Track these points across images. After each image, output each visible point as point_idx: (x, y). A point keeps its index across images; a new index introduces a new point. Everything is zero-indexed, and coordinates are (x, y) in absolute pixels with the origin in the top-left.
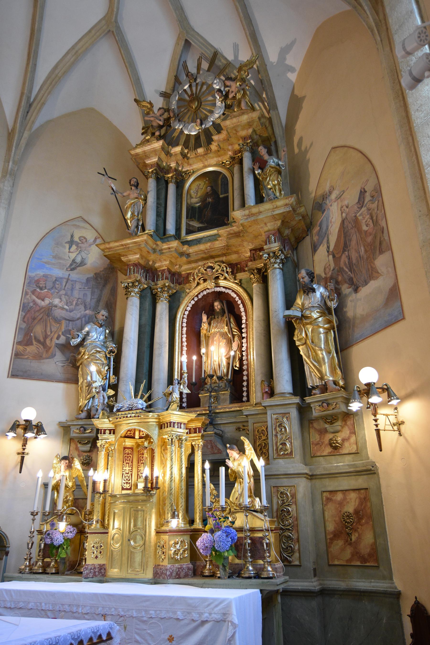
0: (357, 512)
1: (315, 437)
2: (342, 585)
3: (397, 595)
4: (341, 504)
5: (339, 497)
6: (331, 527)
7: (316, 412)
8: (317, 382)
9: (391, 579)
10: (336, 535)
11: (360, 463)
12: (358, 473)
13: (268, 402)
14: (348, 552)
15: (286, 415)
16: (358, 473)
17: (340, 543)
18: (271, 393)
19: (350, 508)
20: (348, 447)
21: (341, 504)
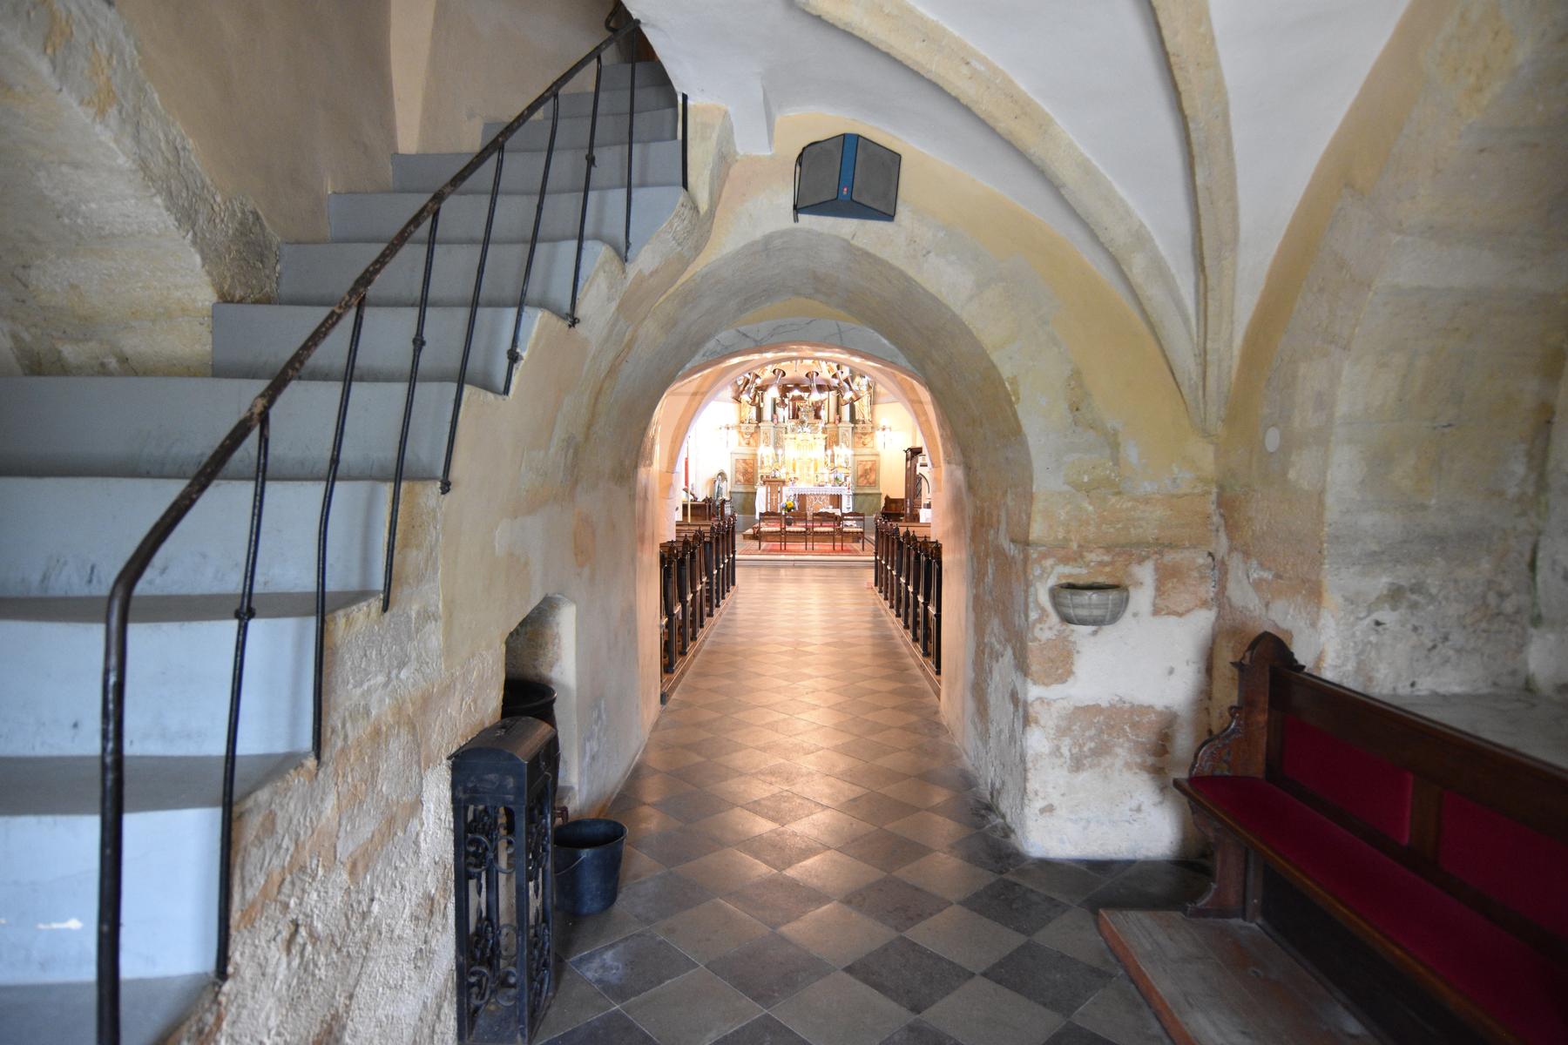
0: (870, 469)
1: (857, 440)
2: (862, 492)
3: (881, 494)
4: (865, 465)
5: (864, 463)
6: (860, 473)
7: (859, 431)
8: (861, 418)
9: (879, 489)
10: (861, 476)
11: (874, 451)
12: (873, 455)
13: (840, 425)
14: (866, 481)
15: (847, 431)
16: (873, 455)
17: (862, 479)
18: (840, 420)
19: (868, 467)
20: (869, 445)
21: (865, 465)
